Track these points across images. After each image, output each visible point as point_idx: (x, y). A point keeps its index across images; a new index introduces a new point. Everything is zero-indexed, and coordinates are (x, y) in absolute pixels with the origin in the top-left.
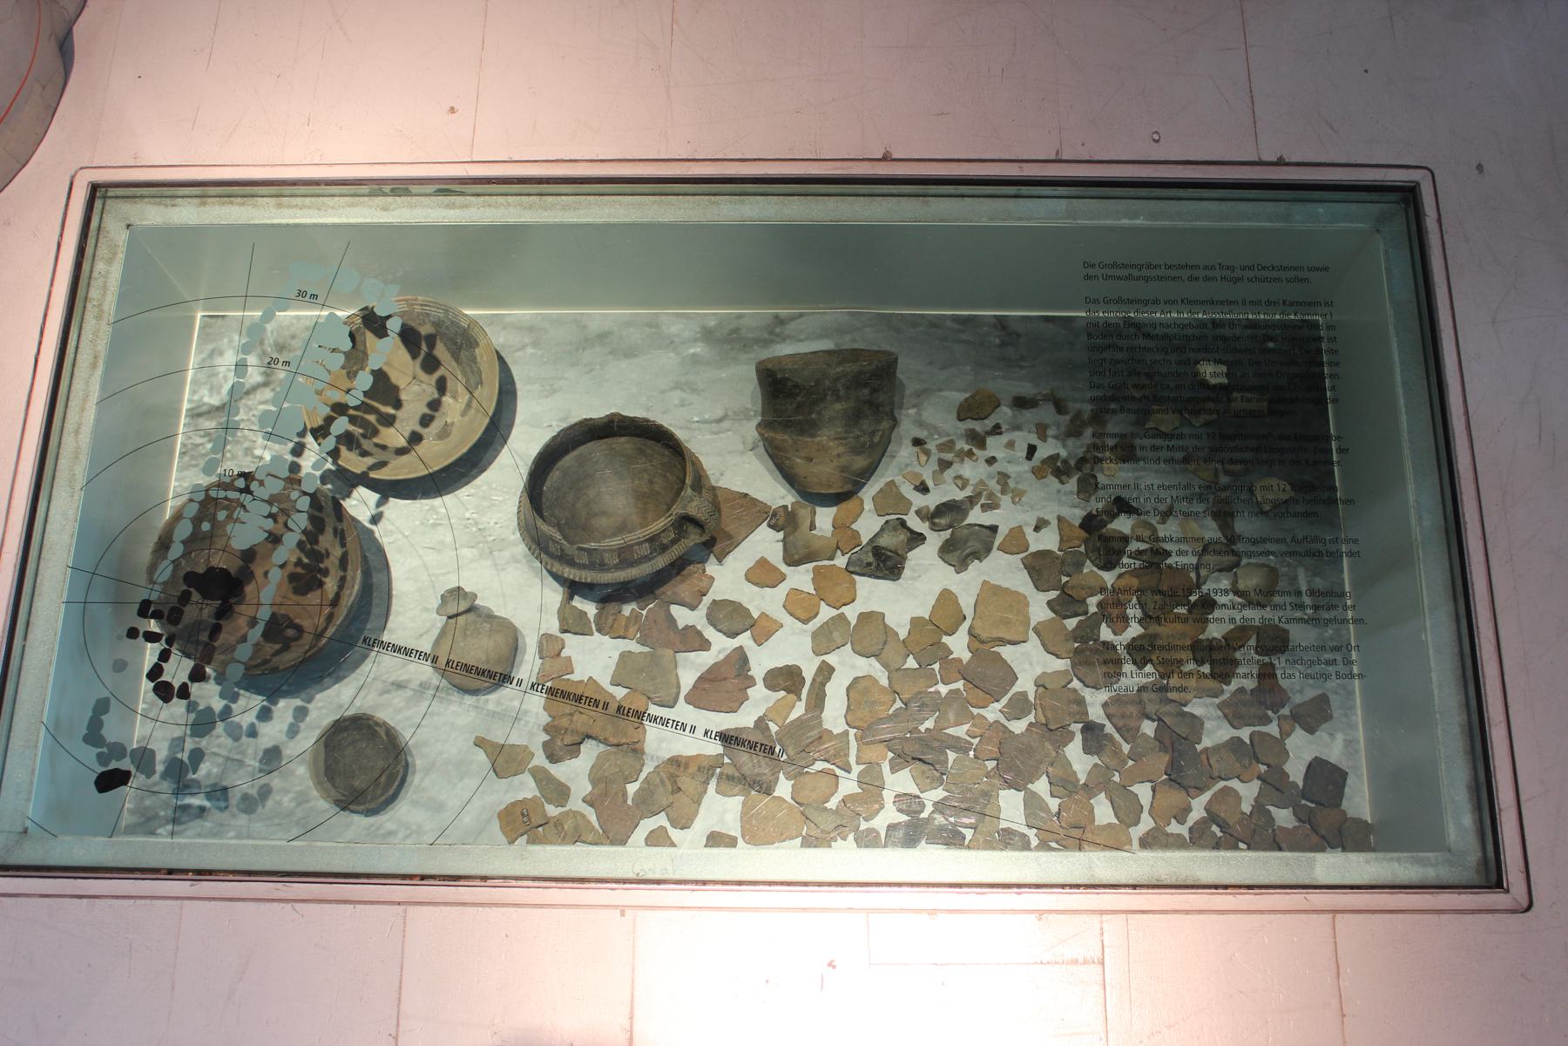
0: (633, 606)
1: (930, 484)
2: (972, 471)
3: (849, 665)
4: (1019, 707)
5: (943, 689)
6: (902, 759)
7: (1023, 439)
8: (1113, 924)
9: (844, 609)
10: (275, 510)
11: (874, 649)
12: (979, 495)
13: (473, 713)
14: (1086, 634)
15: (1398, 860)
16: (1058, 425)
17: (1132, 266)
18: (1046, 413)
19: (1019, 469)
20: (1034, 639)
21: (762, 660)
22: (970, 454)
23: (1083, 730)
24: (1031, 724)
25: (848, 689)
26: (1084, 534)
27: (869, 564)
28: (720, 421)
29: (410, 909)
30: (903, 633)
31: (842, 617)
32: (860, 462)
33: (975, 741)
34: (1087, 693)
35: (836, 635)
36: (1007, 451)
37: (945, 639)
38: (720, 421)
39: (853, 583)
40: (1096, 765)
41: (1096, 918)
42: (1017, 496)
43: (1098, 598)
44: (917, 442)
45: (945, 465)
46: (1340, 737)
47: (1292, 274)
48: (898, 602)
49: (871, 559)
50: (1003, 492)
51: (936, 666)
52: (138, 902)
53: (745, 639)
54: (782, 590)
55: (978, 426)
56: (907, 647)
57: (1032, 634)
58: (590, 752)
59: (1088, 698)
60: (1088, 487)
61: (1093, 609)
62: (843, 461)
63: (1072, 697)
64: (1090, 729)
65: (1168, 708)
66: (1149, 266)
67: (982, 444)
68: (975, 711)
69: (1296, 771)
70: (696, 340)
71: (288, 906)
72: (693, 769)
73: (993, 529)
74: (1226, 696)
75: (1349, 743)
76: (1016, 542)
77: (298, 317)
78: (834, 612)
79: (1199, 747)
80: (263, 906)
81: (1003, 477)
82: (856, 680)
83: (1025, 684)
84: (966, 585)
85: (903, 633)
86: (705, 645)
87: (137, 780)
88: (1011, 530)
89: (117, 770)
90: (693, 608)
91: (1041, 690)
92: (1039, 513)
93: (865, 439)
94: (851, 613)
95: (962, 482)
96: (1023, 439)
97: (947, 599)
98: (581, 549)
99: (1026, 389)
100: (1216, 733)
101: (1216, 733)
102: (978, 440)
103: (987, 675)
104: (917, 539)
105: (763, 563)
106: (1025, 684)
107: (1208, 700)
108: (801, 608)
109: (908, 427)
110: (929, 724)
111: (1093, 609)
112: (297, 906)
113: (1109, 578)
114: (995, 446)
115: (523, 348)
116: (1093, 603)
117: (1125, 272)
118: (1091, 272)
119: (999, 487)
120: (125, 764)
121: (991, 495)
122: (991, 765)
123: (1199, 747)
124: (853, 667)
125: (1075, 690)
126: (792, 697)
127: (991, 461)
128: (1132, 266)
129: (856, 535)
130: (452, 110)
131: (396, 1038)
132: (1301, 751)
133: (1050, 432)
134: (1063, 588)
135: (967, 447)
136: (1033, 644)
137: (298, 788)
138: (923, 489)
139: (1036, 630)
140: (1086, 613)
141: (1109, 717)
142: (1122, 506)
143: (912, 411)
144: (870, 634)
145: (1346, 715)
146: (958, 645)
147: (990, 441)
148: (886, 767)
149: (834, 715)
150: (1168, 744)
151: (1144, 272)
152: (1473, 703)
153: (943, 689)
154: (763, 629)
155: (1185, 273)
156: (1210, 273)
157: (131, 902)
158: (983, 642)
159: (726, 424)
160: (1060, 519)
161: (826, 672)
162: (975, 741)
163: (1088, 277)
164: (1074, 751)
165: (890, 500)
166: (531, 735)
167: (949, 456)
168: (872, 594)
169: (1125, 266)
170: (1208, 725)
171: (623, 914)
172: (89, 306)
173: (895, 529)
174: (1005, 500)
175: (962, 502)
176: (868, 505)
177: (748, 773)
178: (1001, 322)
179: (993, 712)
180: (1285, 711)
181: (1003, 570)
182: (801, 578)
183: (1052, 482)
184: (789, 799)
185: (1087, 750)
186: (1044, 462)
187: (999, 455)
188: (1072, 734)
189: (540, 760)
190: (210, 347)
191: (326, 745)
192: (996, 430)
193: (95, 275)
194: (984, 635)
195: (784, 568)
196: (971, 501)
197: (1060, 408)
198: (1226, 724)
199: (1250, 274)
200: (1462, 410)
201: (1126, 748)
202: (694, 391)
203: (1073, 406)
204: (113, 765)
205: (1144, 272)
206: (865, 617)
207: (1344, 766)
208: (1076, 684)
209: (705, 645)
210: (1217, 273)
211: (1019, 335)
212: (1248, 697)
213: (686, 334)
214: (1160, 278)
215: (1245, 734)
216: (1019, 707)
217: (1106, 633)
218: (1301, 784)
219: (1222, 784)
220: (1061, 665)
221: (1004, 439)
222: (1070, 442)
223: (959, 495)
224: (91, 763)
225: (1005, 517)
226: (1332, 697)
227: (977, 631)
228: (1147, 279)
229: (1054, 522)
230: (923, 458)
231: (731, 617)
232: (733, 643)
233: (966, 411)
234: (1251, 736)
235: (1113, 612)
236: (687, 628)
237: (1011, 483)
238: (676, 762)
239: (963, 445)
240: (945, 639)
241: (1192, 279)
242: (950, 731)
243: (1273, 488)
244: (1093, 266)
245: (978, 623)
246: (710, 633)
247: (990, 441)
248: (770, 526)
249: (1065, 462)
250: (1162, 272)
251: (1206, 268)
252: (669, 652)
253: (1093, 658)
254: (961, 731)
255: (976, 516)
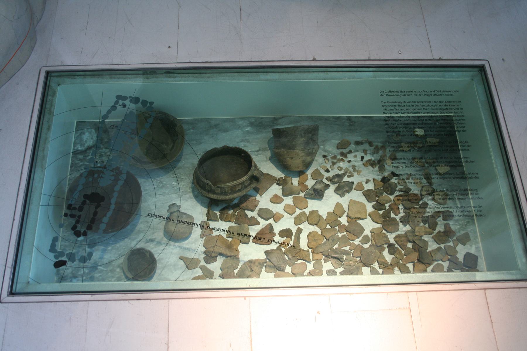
0: (232, 211)
1: (330, 169)
2: (343, 165)
3: (307, 228)
4: (366, 240)
5: (340, 235)
6: (328, 257)
7: (359, 155)
8: (413, 296)
9: (304, 210)
10: (114, 173)
11: (316, 222)
12: (347, 172)
13: (178, 249)
14: (386, 215)
15: (503, 273)
16: (370, 150)
17: (396, 92)
18: (366, 146)
19: (359, 164)
20: (368, 217)
21: (278, 228)
22: (342, 160)
23: (388, 247)
24: (370, 246)
25: (308, 236)
26: (382, 184)
27: (312, 194)
28: (258, 151)
29: (170, 300)
30: (325, 217)
31: (304, 212)
32: (309, 159)
33: (352, 251)
34: (388, 234)
35: (303, 218)
36: (355, 158)
37: (339, 219)
38: (258, 151)
39: (307, 201)
40: (393, 258)
41: (406, 293)
42: (359, 172)
43: (389, 203)
44: (324, 156)
45: (334, 164)
46: (474, 246)
47: (447, 93)
48: (324, 206)
49: (313, 192)
50: (354, 171)
51: (337, 228)
52: (73, 303)
53: (271, 221)
54: (282, 205)
55: (345, 151)
56: (327, 221)
57: (368, 216)
58: (220, 260)
59: (389, 237)
60: (382, 169)
61: (387, 208)
62: (304, 158)
63: (384, 235)
64: (390, 246)
65: (416, 238)
66: (401, 92)
67: (346, 157)
68: (351, 242)
69: (460, 257)
70: (248, 126)
71: (127, 302)
72: (257, 263)
73: (353, 183)
74: (435, 234)
75: (477, 248)
76: (360, 187)
77: (111, 122)
78: (301, 211)
79: (428, 251)
80: (118, 302)
81: (354, 167)
82: (310, 233)
83: (367, 232)
84: (345, 201)
85: (325, 217)
86: (258, 223)
87: (69, 264)
88: (358, 183)
89: (62, 261)
90: (252, 211)
91: (373, 234)
92: (367, 178)
93: (310, 151)
94: (307, 211)
95: (340, 169)
96: (359, 155)
97: (338, 205)
98: (218, 187)
99: (359, 139)
100: (432, 246)
101: (432, 246)
102: (344, 155)
103: (354, 230)
104: (327, 186)
105: (276, 196)
106: (367, 232)
107: (429, 236)
108: (289, 210)
109: (321, 152)
110: (336, 246)
111: (387, 208)
112: (130, 301)
113: (392, 197)
114: (350, 157)
115: (190, 129)
116: (387, 206)
117: (393, 94)
118: (383, 94)
119: (352, 170)
120: (64, 258)
121: (350, 172)
122: (358, 259)
123: (428, 251)
124: (309, 229)
125: (384, 233)
126: (289, 239)
127: (349, 162)
128: (396, 92)
129: (306, 186)
130: (169, 47)
131: (168, 345)
132: (461, 251)
133: (368, 152)
134: (377, 201)
135: (341, 158)
136: (369, 220)
137: (117, 276)
138: (327, 171)
139: (369, 215)
140: (385, 209)
141: (396, 242)
142: (394, 174)
143: (322, 147)
144: (314, 218)
145: (475, 239)
146: (344, 220)
147: (349, 155)
148: (323, 261)
149: (303, 244)
150: (417, 250)
151: (400, 94)
152: (522, 222)
153: (340, 235)
154: (277, 218)
155: (413, 94)
156: (421, 93)
157: (70, 303)
158: (352, 219)
159: (260, 152)
160: (374, 179)
161: (299, 231)
162: (352, 251)
163: (382, 95)
164: (386, 253)
165: (317, 175)
166: (199, 255)
167: (335, 161)
168: (313, 205)
169: (393, 92)
170: (429, 244)
171: (245, 299)
172: (46, 110)
173: (320, 183)
174: (355, 174)
175: (341, 174)
176: (310, 177)
177: (276, 264)
178: (349, 119)
179: (357, 242)
180: (455, 238)
181: (356, 196)
182: (289, 200)
183: (370, 168)
184: (290, 273)
185: (390, 253)
186: (367, 162)
187: (352, 160)
188: (385, 248)
189: (203, 263)
190: (80, 132)
191: (128, 259)
192: (350, 152)
193: (48, 100)
194: (353, 216)
195: (283, 197)
196: (344, 174)
197: (371, 144)
198: (435, 243)
199: (433, 93)
200: (506, 132)
201: (403, 252)
202: (248, 142)
203: (375, 144)
204: (60, 259)
205: (400, 94)
206: (311, 212)
207: (476, 255)
208: (384, 231)
209: (258, 223)
210: (423, 93)
211: (355, 122)
212: (442, 234)
213: (245, 124)
214: (405, 95)
215: (442, 246)
216: (366, 240)
217: (392, 215)
218: (463, 262)
219: (436, 263)
220: (379, 226)
221: (353, 154)
222: (375, 155)
223: (340, 173)
224: (52, 258)
225: (356, 179)
226: (470, 233)
227: (350, 215)
228: (401, 96)
229: (372, 180)
230: (327, 161)
231: (266, 214)
232: (268, 222)
233: (340, 146)
234: (444, 247)
235: (394, 208)
236: (251, 217)
237: (357, 169)
238: (250, 262)
239: (339, 157)
240: (339, 219)
241: (415, 95)
242: (343, 248)
243: (443, 169)
244: (383, 92)
245: (349, 212)
246: (259, 219)
247: (349, 155)
248: (277, 184)
249: (374, 161)
250: (405, 93)
251: (419, 92)
252: (246, 225)
253: (388, 223)
254: (347, 248)
255: (346, 179)
